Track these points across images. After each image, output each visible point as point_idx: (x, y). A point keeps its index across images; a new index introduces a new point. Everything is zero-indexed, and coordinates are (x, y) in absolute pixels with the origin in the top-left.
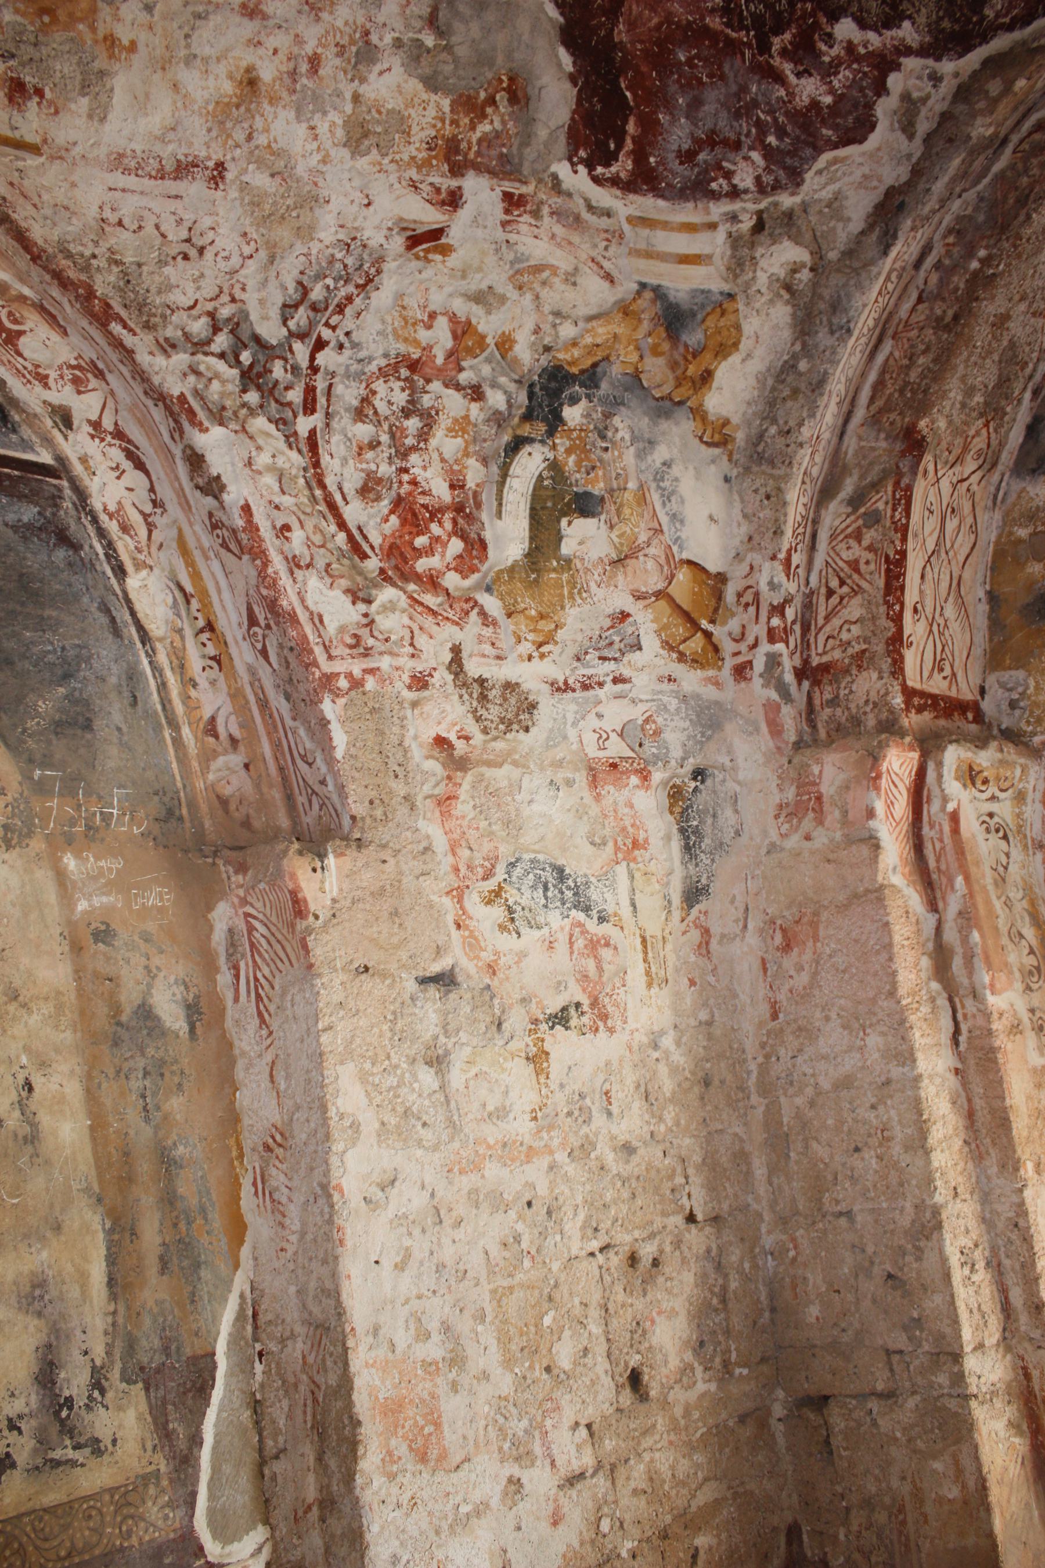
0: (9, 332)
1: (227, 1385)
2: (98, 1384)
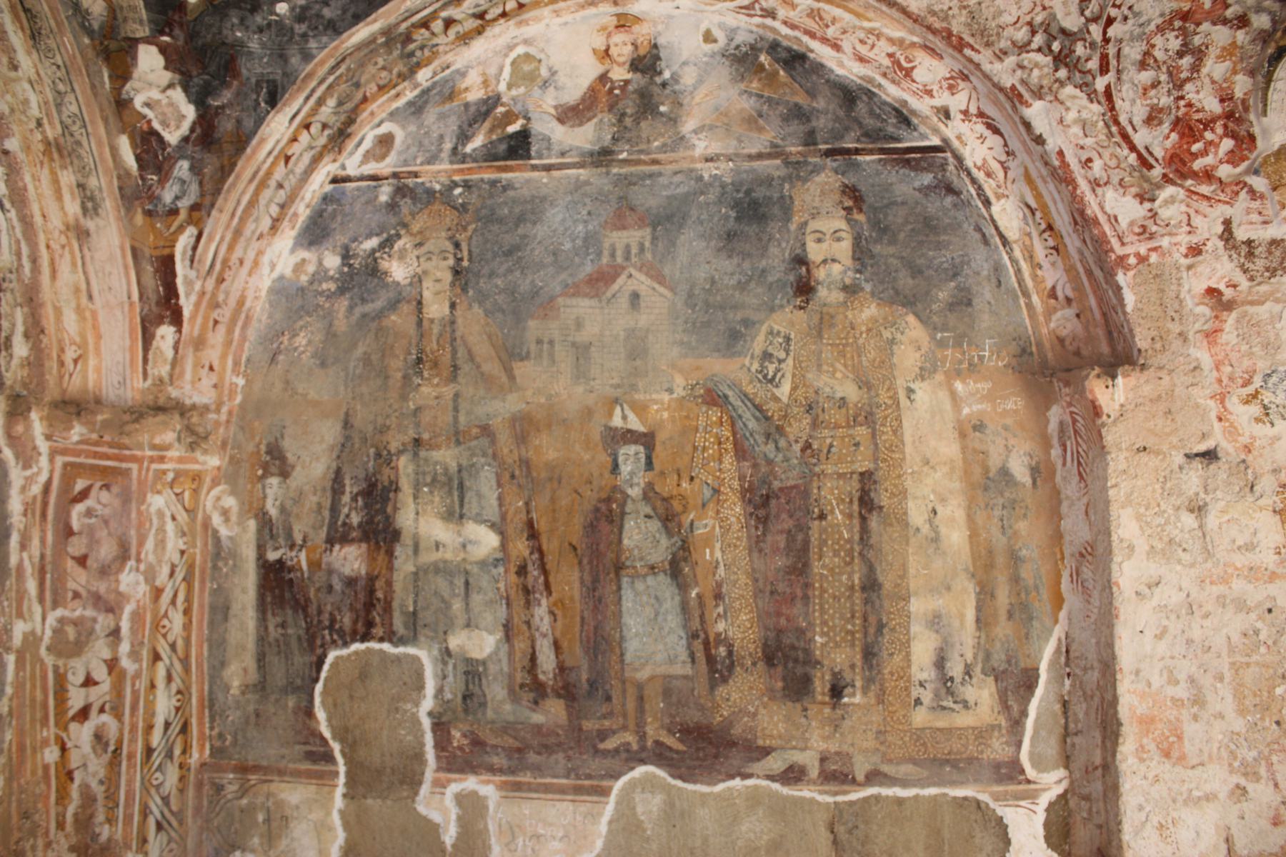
0: (906, 69)
1: (1046, 688)
2: (968, 672)
